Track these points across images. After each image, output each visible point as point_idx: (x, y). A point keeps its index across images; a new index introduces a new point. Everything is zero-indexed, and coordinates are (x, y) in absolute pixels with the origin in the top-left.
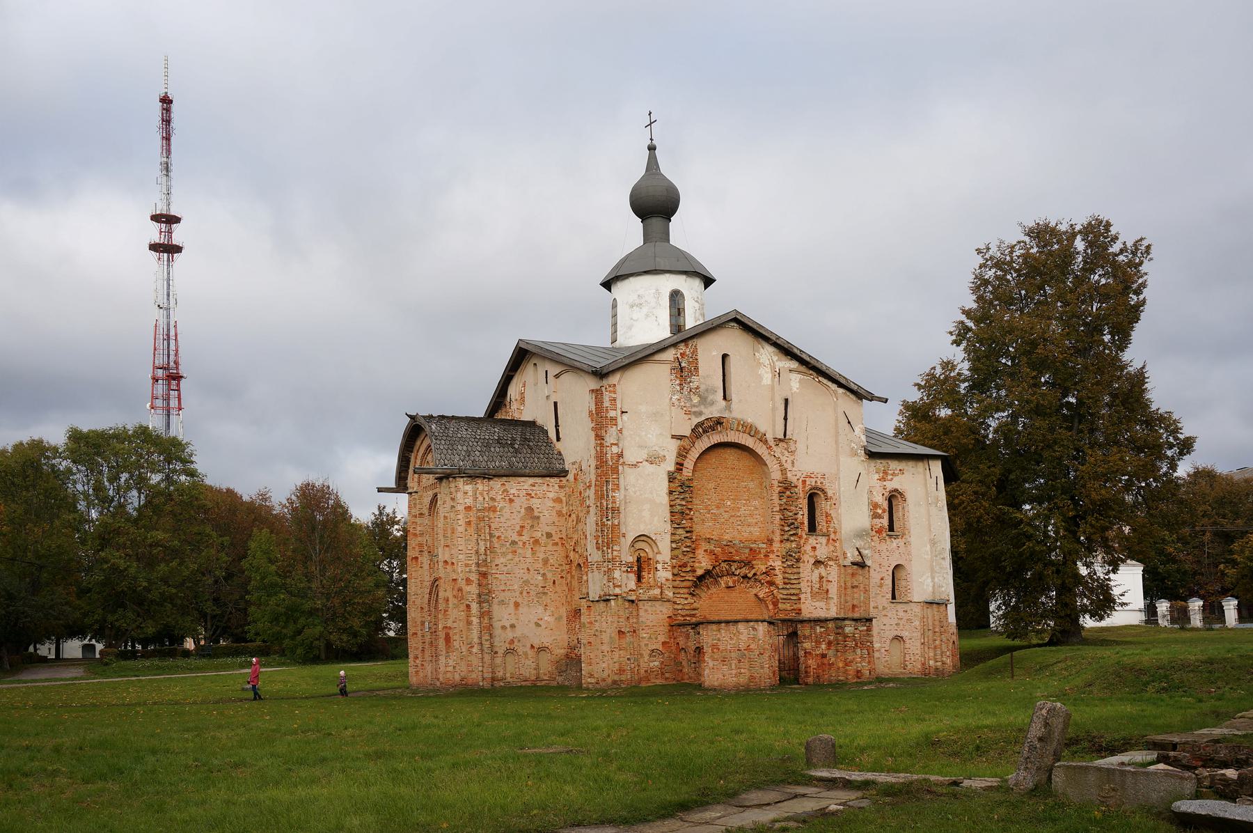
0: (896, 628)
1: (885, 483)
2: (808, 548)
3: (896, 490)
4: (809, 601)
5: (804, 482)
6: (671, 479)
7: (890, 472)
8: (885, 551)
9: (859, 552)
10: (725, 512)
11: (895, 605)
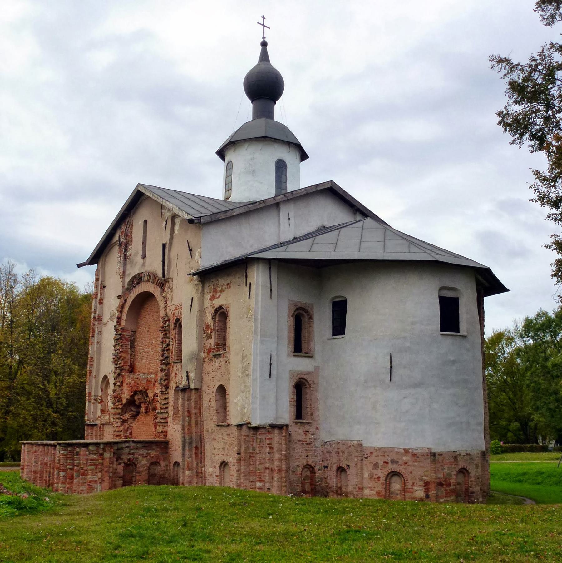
0: (223, 452)
1: (214, 302)
2: (173, 375)
3: (221, 308)
4: (171, 425)
5: (174, 314)
6: (116, 330)
7: (219, 289)
8: (211, 372)
9: (188, 376)
10: (152, 349)
11: (218, 428)
